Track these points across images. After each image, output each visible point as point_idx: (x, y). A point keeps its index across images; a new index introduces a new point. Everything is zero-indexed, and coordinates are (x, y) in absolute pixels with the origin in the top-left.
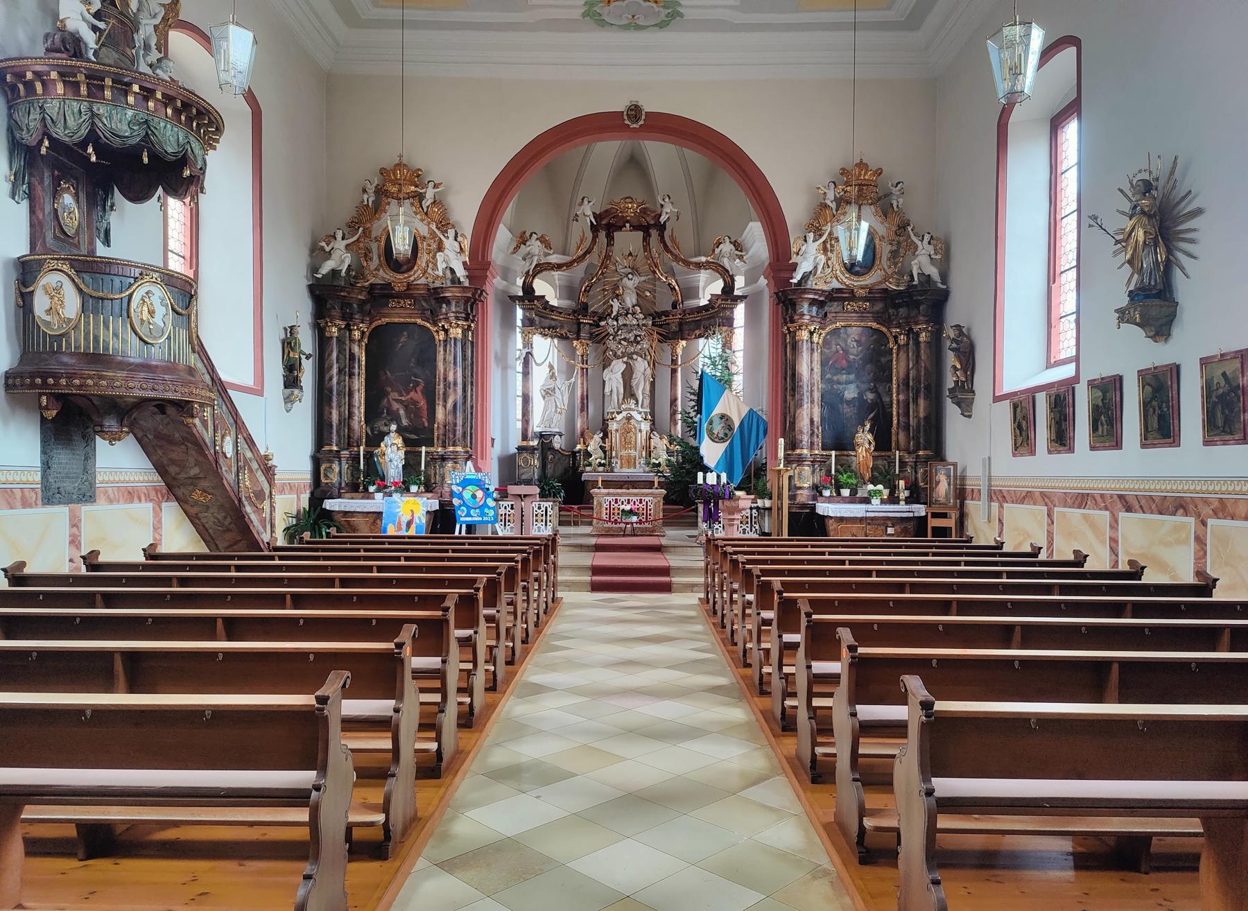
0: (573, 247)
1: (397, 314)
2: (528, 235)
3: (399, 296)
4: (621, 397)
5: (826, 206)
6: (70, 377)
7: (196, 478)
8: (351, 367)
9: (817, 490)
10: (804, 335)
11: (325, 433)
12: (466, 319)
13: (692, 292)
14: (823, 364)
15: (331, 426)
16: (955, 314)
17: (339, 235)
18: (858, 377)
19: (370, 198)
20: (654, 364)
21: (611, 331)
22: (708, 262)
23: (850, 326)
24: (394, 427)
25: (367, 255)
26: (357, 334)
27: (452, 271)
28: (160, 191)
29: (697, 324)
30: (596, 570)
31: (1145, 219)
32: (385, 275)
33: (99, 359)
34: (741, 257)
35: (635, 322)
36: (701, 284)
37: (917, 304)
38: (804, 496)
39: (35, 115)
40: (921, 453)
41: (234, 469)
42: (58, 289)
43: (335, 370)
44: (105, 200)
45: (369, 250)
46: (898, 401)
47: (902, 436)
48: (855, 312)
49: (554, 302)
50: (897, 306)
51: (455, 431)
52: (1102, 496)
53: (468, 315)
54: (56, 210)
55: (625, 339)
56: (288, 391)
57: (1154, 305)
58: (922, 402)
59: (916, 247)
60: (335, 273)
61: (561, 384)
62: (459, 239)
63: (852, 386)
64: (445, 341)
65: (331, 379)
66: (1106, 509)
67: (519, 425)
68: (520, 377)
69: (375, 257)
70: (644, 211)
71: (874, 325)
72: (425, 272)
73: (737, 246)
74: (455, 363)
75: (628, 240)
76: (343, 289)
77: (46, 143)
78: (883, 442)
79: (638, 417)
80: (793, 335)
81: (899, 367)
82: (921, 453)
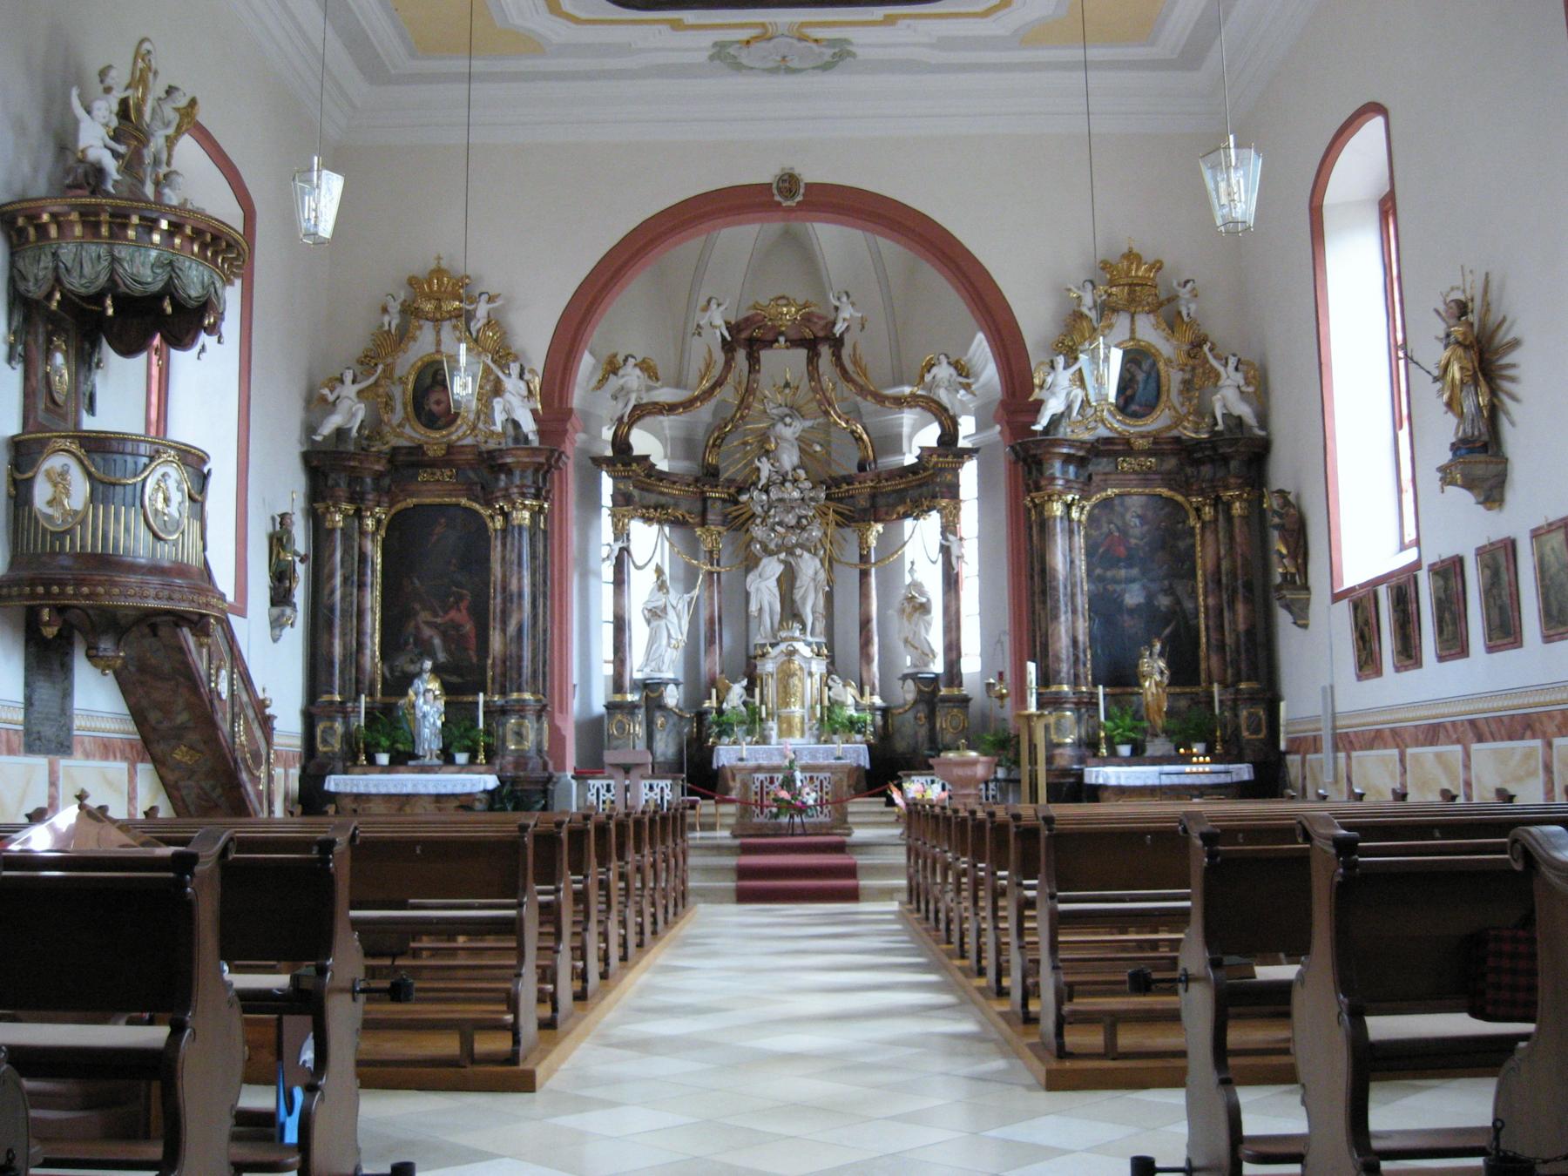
0: (692, 377)
1: (430, 491)
2: (620, 358)
3: (434, 464)
4: (777, 618)
5: (1082, 316)
6: (79, 583)
7: (183, 728)
8: (362, 574)
9: (1089, 747)
10: (1057, 509)
11: (323, 677)
12: (537, 497)
13: (892, 443)
14: (1090, 554)
15: (331, 664)
16: (1281, 474)
17: (349, 377)
18: (1143, 573)
19: (393, 321)
20: (830, 563)
21: (759, 510)
22: (913, 395)
23: (1129, 494)
24: (428, 664)
25: (389, 405)
26: (370, 523)
27: (516, 425)
28: (157, 341)
29: (900, 496)
30: (743, 873)
31: (1460, 351)
32: (414, 433)
33: (107, 563)
34: (967, 387)
35: (796, 494)
36: (906, 430)
37: (1226, 459)
38: (1065, 757)
39: (47, 261)
40: (1243, 686)
41: (229, 716)
42: (63, 474)
43: (338, 580)
44: (91, 355)
45: (390, 397)
46: (1206, 607)
47: (1215, 661)
48: (1135, 472)
49: (663, 465)
50: (1197, 463)
51: (520, 668)
52: (1453, 723)
53: (539, 490)
54: (47, 375)
55: (780, 523)
56: (276, 611)
57: (1480, 461)
58: (1241, 608)
59: (1218, 376)
60: (341, 433)
61: (678, 601)
62: (527, 376)
63: (1136, 587)
64: (504, 530)
65: (332, 592)
66: (1458, 741)
67: (609, 670)
68: (608, 590)
69: (399, 407)
70: (808, 319)
71: (1165, 492)
72: (474, 428)
73: (961, 369)
74: (520, 565)
75: (782, 363)
76: (352, 456)
77: (58, 296)
78: (1183, 670)
79: (805, 650)
80: (1040, 508)
81: (1205, 555)
82: (1243, 686)
